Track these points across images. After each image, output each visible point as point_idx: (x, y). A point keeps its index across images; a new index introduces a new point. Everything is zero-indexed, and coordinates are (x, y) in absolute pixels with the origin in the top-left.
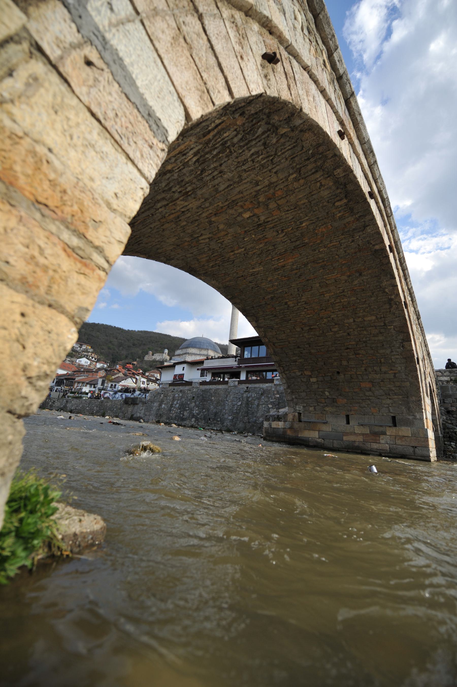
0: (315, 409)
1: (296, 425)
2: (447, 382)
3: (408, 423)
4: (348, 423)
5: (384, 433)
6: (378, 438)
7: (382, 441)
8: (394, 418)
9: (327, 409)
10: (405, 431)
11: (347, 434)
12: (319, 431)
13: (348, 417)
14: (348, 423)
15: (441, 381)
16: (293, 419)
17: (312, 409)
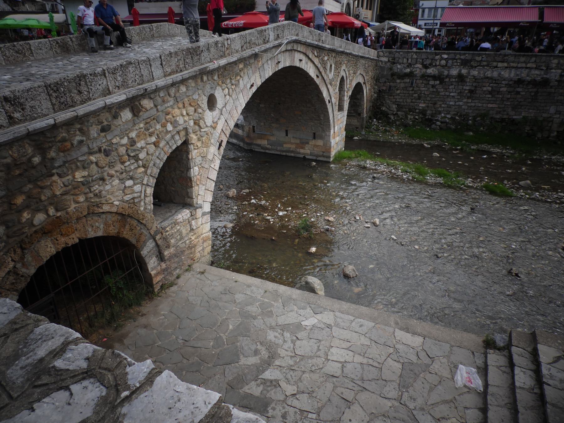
0: (264, 124)
1: (252, 135)
2: (386, 63)
3: (321, 138)
4: (287, 135)
5: (308, 143)
6: (304, 146)
7: (306, 148)
8: (314, 134)
9: (273, 125)
10: (320, 143)
11: (286, 143)
12: (268, 140)
13: (287, 131)
14: (287, 135)
15: (381, 61)
16: (249, 131)
17: (262, 124)
